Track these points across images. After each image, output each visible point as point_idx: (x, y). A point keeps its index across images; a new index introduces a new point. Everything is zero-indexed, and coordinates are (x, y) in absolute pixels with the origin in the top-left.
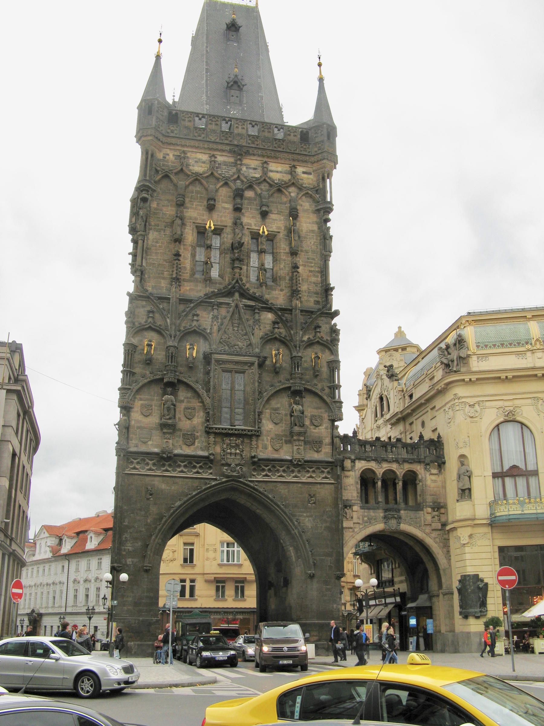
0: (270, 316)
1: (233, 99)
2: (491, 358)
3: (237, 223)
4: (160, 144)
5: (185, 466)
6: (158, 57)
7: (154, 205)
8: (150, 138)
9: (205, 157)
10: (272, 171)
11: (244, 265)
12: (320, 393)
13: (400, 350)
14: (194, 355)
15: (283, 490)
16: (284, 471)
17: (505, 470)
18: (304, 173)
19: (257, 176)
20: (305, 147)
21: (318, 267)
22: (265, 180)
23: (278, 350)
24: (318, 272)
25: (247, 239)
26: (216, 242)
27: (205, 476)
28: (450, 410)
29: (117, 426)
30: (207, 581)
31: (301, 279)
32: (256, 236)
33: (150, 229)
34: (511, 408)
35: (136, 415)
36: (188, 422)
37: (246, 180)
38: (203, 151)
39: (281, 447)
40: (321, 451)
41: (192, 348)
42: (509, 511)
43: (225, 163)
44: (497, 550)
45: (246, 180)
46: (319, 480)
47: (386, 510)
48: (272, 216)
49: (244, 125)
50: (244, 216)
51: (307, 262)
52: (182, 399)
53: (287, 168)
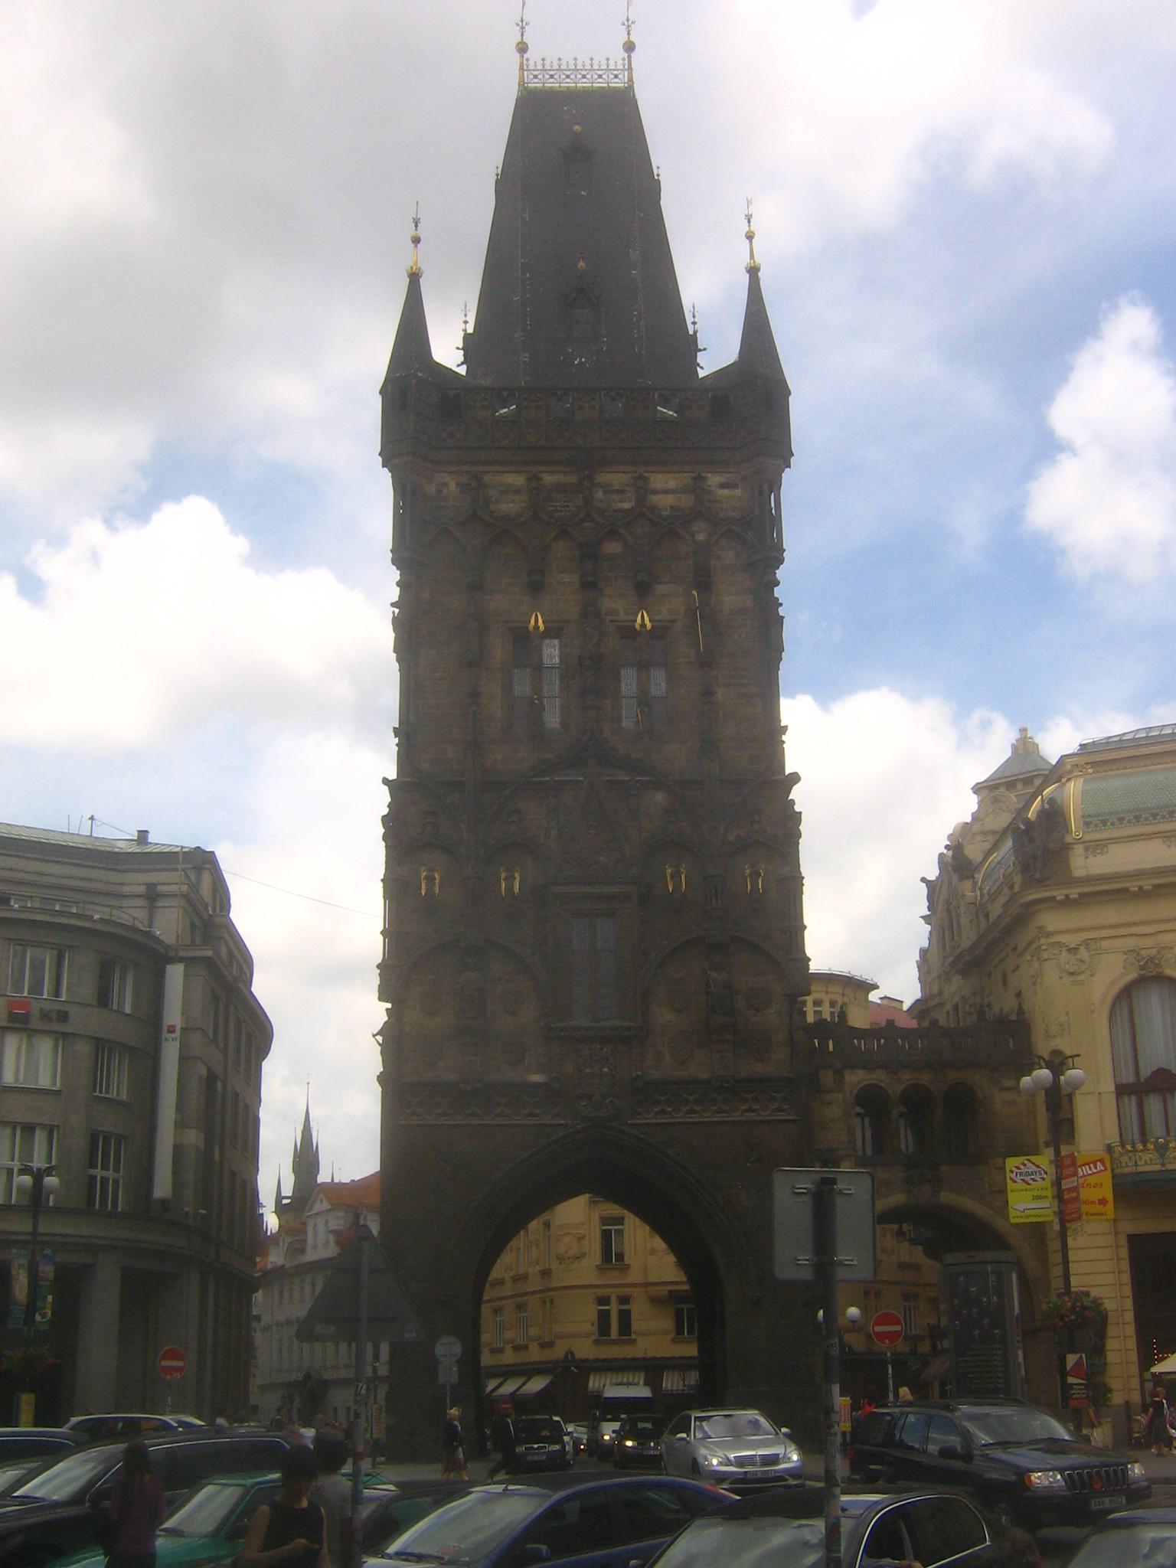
0: (660, 798)
2: (1114, 849)
6: (414, 278)
9: (517, 480)
10: (656, 492)
13: (1020, 786)
14: (516, 889)
17: (1142, 1080)
18: (722, 486)
19: (626, 506)
26: (551, 653)
28: (1035, 959)
29: (380, 1038)
30: (655, 1301)
31: (721, 712)
32: (629, 633)
34: (1154, 951)
41: (510, 879)
42: (1136, 1165)
44: (1123, 1240)
48: (661, 589)
53: (685, 478)
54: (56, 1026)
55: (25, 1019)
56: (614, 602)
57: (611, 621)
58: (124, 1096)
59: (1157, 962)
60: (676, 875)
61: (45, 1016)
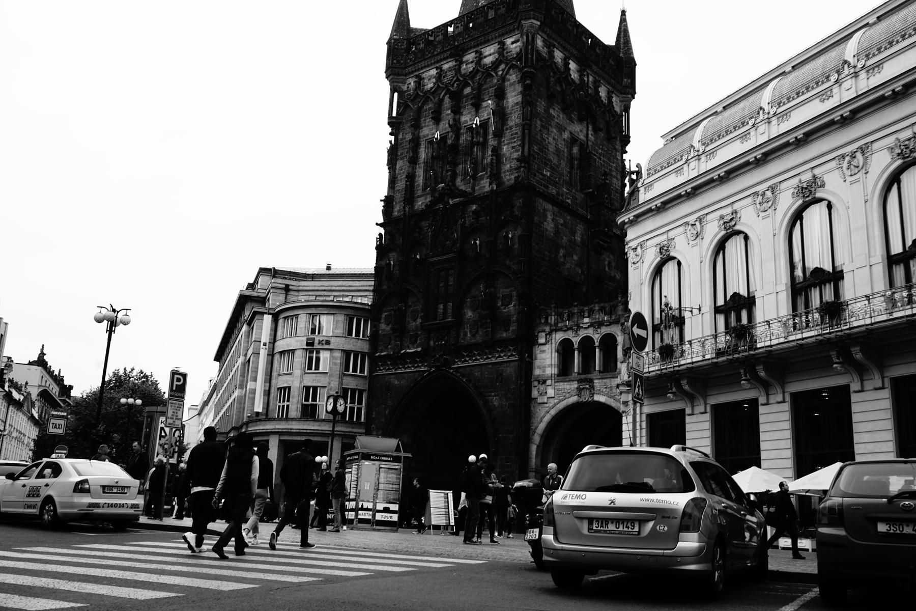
2: (656, 185)
3: (456, 127)
5: (410, 363)
7: (400, 137)
10: (485, 57)
11: (460, 164)
12: (506, 273)
15: (477, 373)
16: (479, 355)
18: (513, 43)
19: (471, 69)
20: (512, 14)
21: (520, 140)
22: (478, 70)
23: (475, 240)
24: (519, 145)
25: (464, 138)
27: (423, 369)
32: (470, 129)
33: (396, 161)
34: (666, 243)
35: (383, 326)
36: (414, 323)
37: (461, 79)
38: (433, 67)
39: (477, 332)
40: (509, 329)
43: (450, 69)
44: (644, 417)
45: (461, 79)
46: (506, 359)
47: (580, 381)
48: (484, 104)
49: (462, 21)
50: (462, 115)
51: (511, 139)
52: (410, 304)
54: (326, 347)
55: (312, 344)
56: (465, 118)
57: (465, 126)
58: (366, 374)
59: (665, 248)
60: (475, 243)
61: (320, 342)
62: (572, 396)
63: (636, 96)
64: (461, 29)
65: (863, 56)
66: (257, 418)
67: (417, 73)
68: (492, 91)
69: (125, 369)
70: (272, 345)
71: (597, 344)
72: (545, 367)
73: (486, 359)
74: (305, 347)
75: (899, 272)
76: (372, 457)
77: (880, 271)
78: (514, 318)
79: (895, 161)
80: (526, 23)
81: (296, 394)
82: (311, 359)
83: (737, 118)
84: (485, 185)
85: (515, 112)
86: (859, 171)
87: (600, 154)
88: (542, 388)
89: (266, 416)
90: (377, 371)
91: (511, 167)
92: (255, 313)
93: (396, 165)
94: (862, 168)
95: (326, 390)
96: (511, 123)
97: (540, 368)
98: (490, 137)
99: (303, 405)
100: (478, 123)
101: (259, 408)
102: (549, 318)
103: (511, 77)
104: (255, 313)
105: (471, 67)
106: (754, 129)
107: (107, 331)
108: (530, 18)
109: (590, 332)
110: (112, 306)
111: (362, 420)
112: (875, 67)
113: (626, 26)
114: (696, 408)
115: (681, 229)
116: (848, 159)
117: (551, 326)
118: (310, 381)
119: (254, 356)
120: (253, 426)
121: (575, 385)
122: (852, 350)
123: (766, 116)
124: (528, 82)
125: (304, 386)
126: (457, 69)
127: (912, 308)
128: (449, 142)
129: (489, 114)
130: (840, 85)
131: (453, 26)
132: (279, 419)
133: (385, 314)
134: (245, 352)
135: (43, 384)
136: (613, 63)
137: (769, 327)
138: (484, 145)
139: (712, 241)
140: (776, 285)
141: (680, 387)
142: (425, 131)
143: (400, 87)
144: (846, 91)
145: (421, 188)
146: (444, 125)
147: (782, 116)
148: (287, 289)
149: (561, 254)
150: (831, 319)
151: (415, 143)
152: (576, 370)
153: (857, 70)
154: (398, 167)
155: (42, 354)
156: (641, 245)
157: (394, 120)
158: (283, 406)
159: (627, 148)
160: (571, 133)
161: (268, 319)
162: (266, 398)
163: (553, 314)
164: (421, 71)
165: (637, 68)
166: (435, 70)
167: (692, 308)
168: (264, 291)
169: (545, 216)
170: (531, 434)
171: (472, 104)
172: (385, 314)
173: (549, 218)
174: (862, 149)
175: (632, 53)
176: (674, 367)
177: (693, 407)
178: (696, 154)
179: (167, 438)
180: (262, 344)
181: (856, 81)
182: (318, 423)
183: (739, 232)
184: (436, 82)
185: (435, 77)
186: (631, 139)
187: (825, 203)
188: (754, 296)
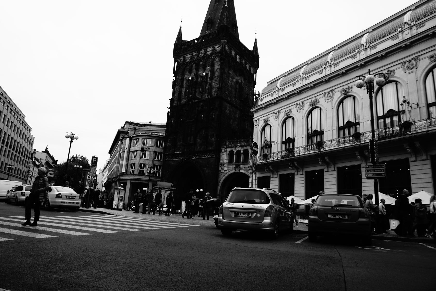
1: (209, 28)
3: (197, 75)
4: (179, 57)
6: (181, 27)
7: (177, 78)
8: (175, 57)
9: (190, 56)
10: (208, 52)
16: (201, 155)
18: (218, 47)
19: (203, 55)
22: (205, 56)
25: (199, 79)
27: (182, 159)
32: (202, 76)
33: (175, 86)
34: (267, 119)
35: (168, 144)
36: (179, 143)
43: (195, 55)
46: (211, 157)
47: (236, 165)
48: (207, 68)
50: (199, 71)
51: (216, 81)
54: (148, 150)
55: (143, 149)
59: (266, 121)
61: (146, 148)
62: (233, 170)
63: (259, 68)
64: (200, 41)
65: (333, 60)
66: (123, 174)
67: (184, 56)
68: (210, 63)
69: (76, 155)
70: (129, 149)
71: (242, 153)
72: (224, 160)
73: (204, 156)
74: (141, 150)
75: (341, 132)
76: (162, 189)
77: (335, 132)
78: (214, 143)
79: (342, 96)
80: (222, 41)
81: (137, 166)
82: (143, 154)
83: (292, 78)
84: (206, 96)
85: (217, 71)
86: (330, 98)
87: (246, 87)
88: (223, 167)
89: (126, 173)
90: (166, 159)
91: (215, 90)
92: (124, 137)
93: (175, 88)
94: (331, 97)
95: (148, 165)
96: (216, 75)
97: (222, 160)
98: (208, 80)
99: (139, 170)
100: (205, 74)
101: (124, 170)
102: (226, 143)
103: (216, 59)
104: (124, 137)
105: (203, 55)
106: (297, 82)
107: (70, 141)
108: (224, 39)
109: (240, 149)
110: (72, 133)
111: (160, 176)
112: (337, 64)
113: (256, 44)
114: (274, 175)
115: (272, 115)
116: (327, 94)
117: (227, 146)
118: (142, 162)
119: (123, 152)
120: (121, 177)
121: (234, 166)
122: (325, 158)
123: (301, 78)
124: (222, 61)
125: (140, 164)
126: (198, 55)
127: (345, 145)
128: (194, 80)
129: (208, 72)
130: (325, 69)
131: (197, 40)
132: (131, 175)
133: (169, 139)
134: (120, 151)
135: (47, 159)
136: (251, 56)
137: (299, 149)
138: (206, 82)
139: (282, 119)
140: (302, 135)
141: (269, 168)
142: (186, 76)
143: (178, 60)
144: (327, 72)
145: (184, 96)
146: (193, 75)
147: (307, 78)
148: (135, 129)
149: (231, 121)
150: (319, 147)
151: (182, 80)
152: (234, 161)
153: (331, 64)
154: (176, 88)
155: (47, 149)
156: (258, 119)
157: (175, 72)
158: (132, 170)
159: (255, 86)
160: (236, 80)
161: (128, 139)
162: (127, 167)
163: (228, 142)
164: (186, 55)
165: (260, 59)
166: (190, 55)
167: (274, 142)
168: (127, 130)
169: (226, 108)
170: (218, 182)
171: (202, 68)
172: (169, 139)
173: (228, 108)
174: (332, 91)
175: (258, 53)
176: (267, 161)
177: (273, 175)
178: (278, 89)
179: (90, 180)
180: (126, 148)
181: (331, 68)
182: (144, 177)
183: (291, 117)
184: (191, 59)
185: (190, 58)
186: (256, 83)
187: (319, 108)
188: (295, 138)
